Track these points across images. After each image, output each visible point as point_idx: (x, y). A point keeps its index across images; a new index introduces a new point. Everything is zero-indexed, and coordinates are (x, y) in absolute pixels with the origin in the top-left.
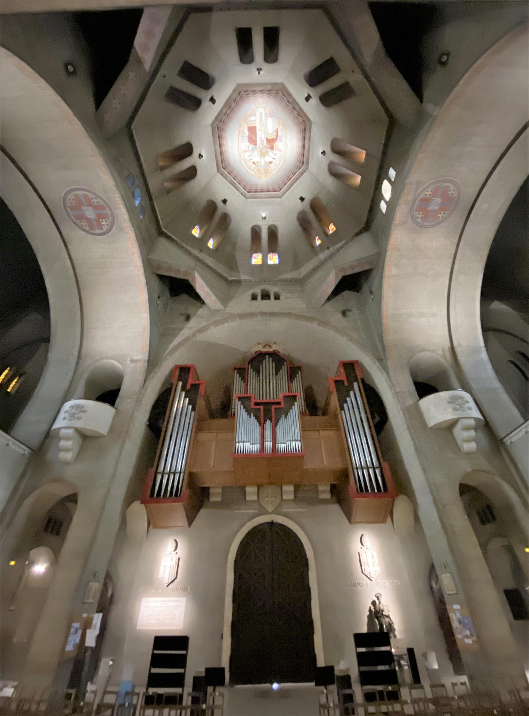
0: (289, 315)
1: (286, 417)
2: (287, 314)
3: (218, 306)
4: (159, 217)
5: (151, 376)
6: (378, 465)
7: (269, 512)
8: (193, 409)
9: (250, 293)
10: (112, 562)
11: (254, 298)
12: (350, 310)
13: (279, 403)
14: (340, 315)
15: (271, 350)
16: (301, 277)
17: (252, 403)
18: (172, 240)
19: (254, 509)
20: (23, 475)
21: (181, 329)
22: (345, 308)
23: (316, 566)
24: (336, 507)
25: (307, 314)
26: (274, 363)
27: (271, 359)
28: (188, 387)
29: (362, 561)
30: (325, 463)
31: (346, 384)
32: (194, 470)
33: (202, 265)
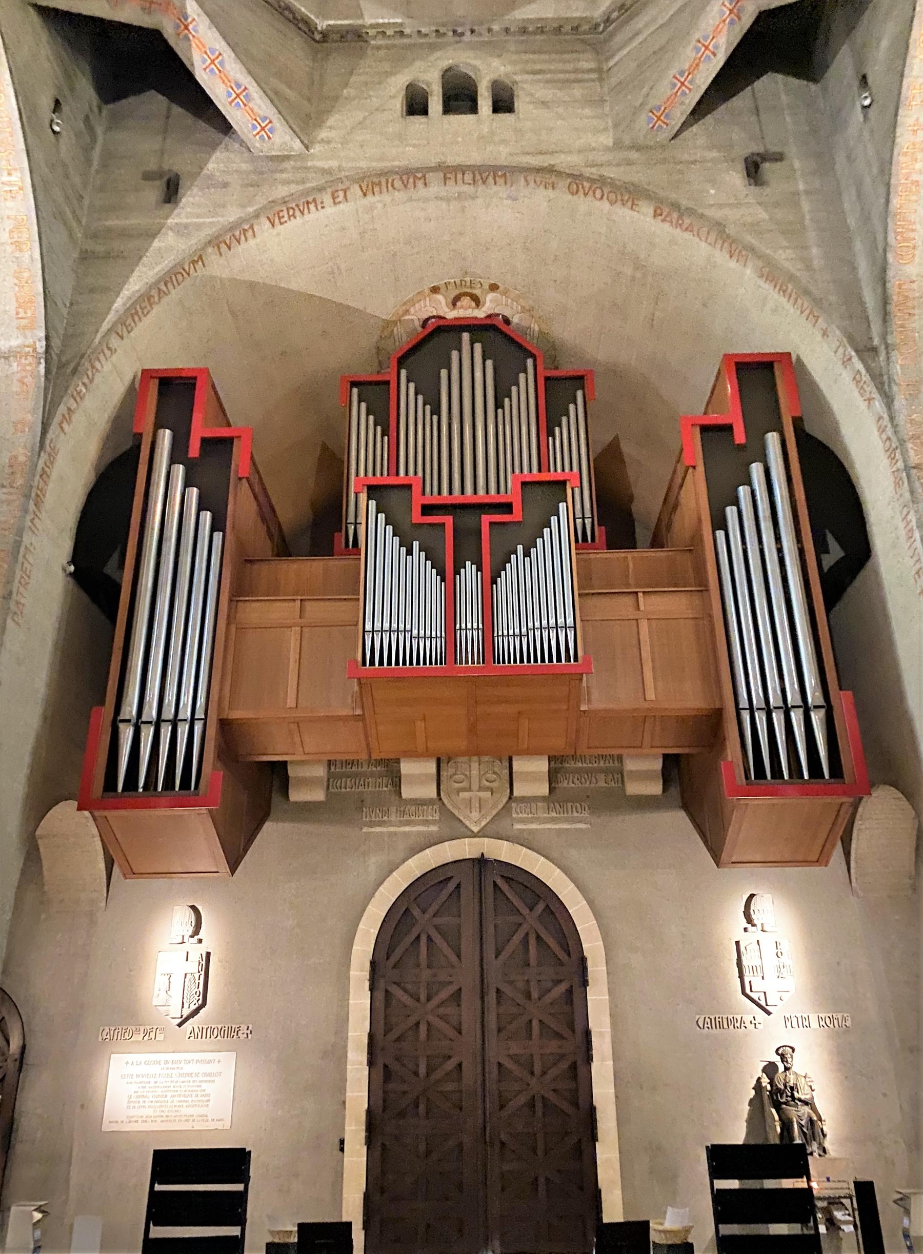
1: (527, 554)
2: (539, 170)
5: (62, 409)
6: (821, 701)
7: (473, 832)
9: (398, 83)
12: (778, 157)
13: (507, 508)
14: (736, 178)
15: (480, 314)
21: (152, 234)
24: (679, 820)
25: (610, 173)
26: (489, 363)
27: (478, 347)
28: (194, 450)
29: (745, 962)
30: (651, 695)
31: (740, 437)
32: (236, 714)
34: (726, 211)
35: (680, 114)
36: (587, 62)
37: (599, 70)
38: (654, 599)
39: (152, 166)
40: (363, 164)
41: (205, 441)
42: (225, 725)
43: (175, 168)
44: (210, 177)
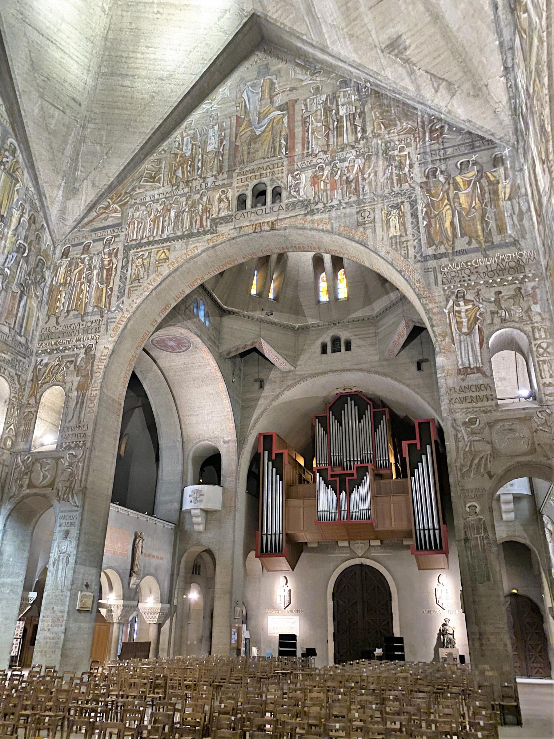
0: (361, 370)
2: (358, 370)
3: (289, 367)
4: (219, 301)
8: (281, 479)
9: (319, 343)
10: (244, 595)
11: (324, 350)
12: (427, 360)
13: (352, 475)
17: (329, 476)
18: (234, 313)
19: (346, 553)
20: (175, 541)
22: (421, 358)
23: (398, 597)
25: (379, 369)
27: (353, 402)
28: (274, 458)
30: (393, 526)
32: (289, 532)
33: (265, 325)
38: (395, 497)
39: (256, 377)
40: (310, 372)
42: (287, 535)
43: (262, 377)
44: (271, 380)
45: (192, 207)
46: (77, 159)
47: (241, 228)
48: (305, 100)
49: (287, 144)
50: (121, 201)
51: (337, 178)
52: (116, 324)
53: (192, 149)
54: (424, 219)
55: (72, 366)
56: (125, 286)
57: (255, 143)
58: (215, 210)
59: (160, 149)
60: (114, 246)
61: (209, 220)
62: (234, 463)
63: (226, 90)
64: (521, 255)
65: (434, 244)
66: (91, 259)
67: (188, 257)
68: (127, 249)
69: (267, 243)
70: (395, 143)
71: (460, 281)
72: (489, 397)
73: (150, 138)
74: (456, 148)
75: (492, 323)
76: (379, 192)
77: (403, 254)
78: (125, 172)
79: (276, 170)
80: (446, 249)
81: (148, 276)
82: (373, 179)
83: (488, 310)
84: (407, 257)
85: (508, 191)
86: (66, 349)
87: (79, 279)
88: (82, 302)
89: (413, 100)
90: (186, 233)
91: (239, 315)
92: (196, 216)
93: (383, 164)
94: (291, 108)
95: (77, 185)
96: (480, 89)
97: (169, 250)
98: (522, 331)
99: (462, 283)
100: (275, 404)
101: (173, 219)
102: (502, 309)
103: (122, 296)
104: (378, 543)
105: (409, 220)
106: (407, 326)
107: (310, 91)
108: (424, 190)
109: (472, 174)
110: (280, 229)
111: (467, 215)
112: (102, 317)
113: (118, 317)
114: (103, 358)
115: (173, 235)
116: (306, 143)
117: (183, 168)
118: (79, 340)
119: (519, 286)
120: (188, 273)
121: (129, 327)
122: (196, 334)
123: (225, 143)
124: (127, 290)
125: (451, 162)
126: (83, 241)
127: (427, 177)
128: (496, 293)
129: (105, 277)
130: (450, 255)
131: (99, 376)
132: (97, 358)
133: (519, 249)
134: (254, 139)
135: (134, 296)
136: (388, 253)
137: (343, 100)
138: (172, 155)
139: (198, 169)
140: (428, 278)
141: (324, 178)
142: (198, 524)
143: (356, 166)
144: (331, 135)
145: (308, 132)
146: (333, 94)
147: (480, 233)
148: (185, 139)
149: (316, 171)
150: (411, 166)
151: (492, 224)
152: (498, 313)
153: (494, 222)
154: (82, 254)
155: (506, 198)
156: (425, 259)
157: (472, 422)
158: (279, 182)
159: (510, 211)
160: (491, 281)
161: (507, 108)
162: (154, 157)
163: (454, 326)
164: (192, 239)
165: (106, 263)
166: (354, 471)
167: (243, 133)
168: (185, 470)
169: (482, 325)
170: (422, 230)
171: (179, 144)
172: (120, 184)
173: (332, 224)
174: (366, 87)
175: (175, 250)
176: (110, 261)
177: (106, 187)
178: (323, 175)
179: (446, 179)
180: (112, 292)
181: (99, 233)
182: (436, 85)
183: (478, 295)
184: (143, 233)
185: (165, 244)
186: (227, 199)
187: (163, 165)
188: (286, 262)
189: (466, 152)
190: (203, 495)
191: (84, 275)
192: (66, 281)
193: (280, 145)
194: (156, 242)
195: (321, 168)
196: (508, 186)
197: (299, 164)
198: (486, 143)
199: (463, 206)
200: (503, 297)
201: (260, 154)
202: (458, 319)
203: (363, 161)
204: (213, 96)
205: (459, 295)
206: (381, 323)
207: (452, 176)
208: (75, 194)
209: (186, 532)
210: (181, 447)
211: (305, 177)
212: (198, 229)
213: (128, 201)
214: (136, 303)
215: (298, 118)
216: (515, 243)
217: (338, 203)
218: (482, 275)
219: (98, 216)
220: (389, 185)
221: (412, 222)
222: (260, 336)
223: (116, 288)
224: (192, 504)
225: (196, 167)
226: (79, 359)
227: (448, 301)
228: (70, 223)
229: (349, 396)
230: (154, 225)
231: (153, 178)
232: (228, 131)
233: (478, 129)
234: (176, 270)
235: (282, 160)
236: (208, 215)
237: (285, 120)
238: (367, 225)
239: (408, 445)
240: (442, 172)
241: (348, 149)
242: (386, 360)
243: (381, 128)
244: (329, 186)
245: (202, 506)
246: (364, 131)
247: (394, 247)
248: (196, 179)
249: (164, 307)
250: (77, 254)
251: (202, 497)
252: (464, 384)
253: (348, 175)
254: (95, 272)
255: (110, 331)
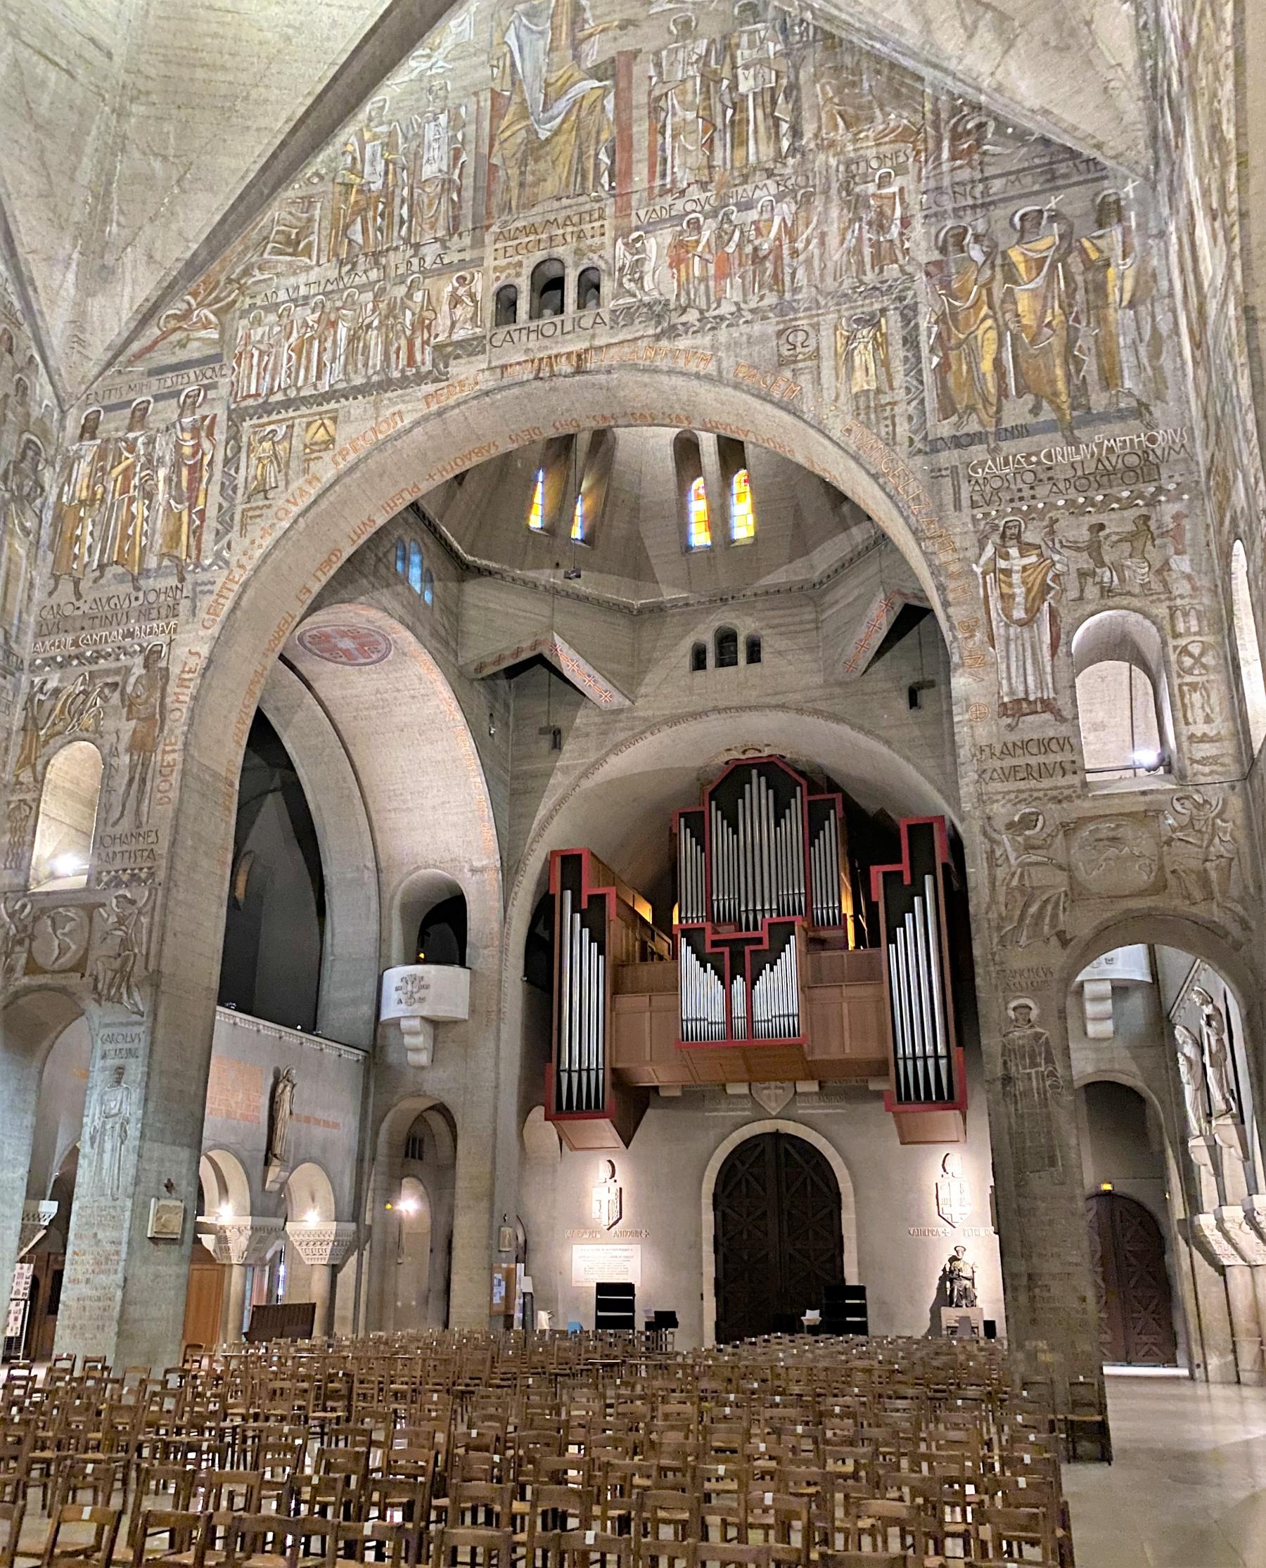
0: (783, 707)
3: (618, 700)
4: (456, 544)
8: (601, 951)
11: (699, 661)
12: (931, 684)
13: (759, 941)
14: (903, 703)
16: (816, 576)
18: (490, 573)
22: (917, 678)
25: (821, 705)
27: (763, 779)
28: (584, 905)
32: (619, 1065)
33: (565, 602)
34: (893, 731)
35: (863, 665)
36: (808, 614)
37: (816, 621)
39: (544, 724)
41: (591, 897)
42: (614, 1071)
45: (387, 317)
46: (108, 193)
47: (504, 368)
48: (657, 53)
49: (613, 162)
50: (217, 300)
51: (731, 249)
52: (214, 597)
53: (386, 173)
54: (932, 350)
55: (117, 695)
56: (233, 506)
57: (536, 161)
58: (443, 323)
59: (309, 172)
60: (205, 411)
61: (428, 349)
62: (497, 915)
63: (466, 24)
64: (1152, 440)
65: (954, 411)
66: (151, 442)
67: (381, 437)
68: (236, 417)
69: (567, 404)
70: (868, 166)
71: (1012, 500)
72: (1068, 766)
73: (283, 144)
74: (1012, 178)
75: (1081, 598)
76: (830, 284)
77: (883, 434)
78: (226, 227)
79: (587, 227)
80: (981, 422)
81: (287, 483)
82: (817, 252)
83: (1073, 568)
84: (891, 441)
85: (1129, 284)
86: (98, 655)
87: (125, 490)
88: (133, 544)
89: (914, 55)
90: (375, 378)
91: (503, 578)
92: (398, 338)
93: (840, 217)
94: (623, 71)
95: (109, 259)
96: (1073, 33)
97: (334, 420)
98: (1146, 615)
99: (1016, 504)
100: (587, 784)
101: (343, 344)
102: (1103, 564)
103: (228, 532)
104: (814, 1087)
105: (898, 352)
106: (890, 605)
107: (670, 32)
108: (935, 280)
109: (1046, 242)
110: (598, 372)
111: (1033, 342)
112: (182, 580)
113: (220, 582)
114: (186, 676)
115: (344, 385)
116: (657, 162)
117: (365, 222)
118: (131, 634)
119: (1144, 511)
120: (381, 476)
121: (244, 603)
122: (402, 621)
123: (464, 158)
124: (237, 517)
125: (999, 213)
126: (131, 396)
127: (943, 250)
128: (1091, 528)
129: (184, 484)
130: (991, 439)
131: (178, 719)
132: (172, 677)
133: (1150, 426)
134: (534, 149)
135: (255, 530)
136: (849, 431)
137: (747, 53)
138: (338, 188)
139: (402, 222)
140: (939, 491)
141: (700, 249)
142: (416, 1050)
143: (777, 220)
144: (717, 143)
145: (663, 134)
146: (724, 38)
147: (1061, 385)
148: (368, 148)
149: (681, 233)
150: (906, 222)
151: (1090, 366)
152: (1094, 574)
153: (1094, 362)
154: (130, 429)
155: (1125, 303)
156: (934, 446)
157: (1027, 822)
158: (595, 257)
159: (1132, 334)
160: (1081, 500)
161: (1135, 79)
162: (294, 191)
163: (995, 605)
164: (389, 394)
165: (187, 451)
166: (763, 933)
167: (508, 133)
168: (385, 935)
169: (1059, 601)
170: (927, 377)
171: (354, 159)
172: (213, 259)
173: (719, 361)
174: (802, 21)
175: (348, 420)
176: (197, 447)
177: (180, 265)
178: (698, 242)
179: (988, 255)
180: (202, 521)
181: (169, 379)
182: (969, 20)
183: (1052, 532)
184: (273, 380)
185: (326, 407)
186: (472, 296)
187: (317, 213)
188: (611, 450)
189: (1037, 187)
190: (427, 987)
191: (136, 481)
192: (94, 494)
193: (597, 166)
194: (305, 401)
195: (696, 226)
196: (1130, 274)
197: (642, 213)
198: (1082, 167)
199: (1025, 321)
200: (1108, 536)
201: (550, 186)
202: (1006, 590)
203: (794, 208)
204: (433, 38)
205: (1008, 532)
206: (828, 599)
207: (1001, 248)
208: (106, 281)
209: (389, 1067)
210: (374, 881)
211: (656, 246)
212: (403, 371)
213: (234, 302)
214: (260, 546)
215: (640, 97)
216: (1141, 411)
217: (734, 309)
218: (1061, 485)
219: (165, 336)
220: (854, 268)
221: (906, 359)
222: (551, 628)
223: (212, 512)
224: (403, 1006)
225: (397, 219)
226: (132, 680)
227: (982, 549)
228: (98, 351)
229: (753, 766)
230: (299, 358)
231: (293, 244)
232: (471, 129)
233: (1065, 131)
234: (351, 470)
235: (601, 204)
236: (426, 335)
237: (610, 103)
238: (801, 365)
239: (885, 874)
240: (977, 238)
241: (759, 177)
242: (840, 684)
243: (836, 126)
244: (712, 268)
245: (426, 1011)
246: (796, 132)
247: (862, 417)
248: (397, 248)
249: (326, 556)
250: (117, 430)
251: (423, 993)
252: (1011, 738)
253: (757, 242)
254: (162, 473)
255: (202, 615)
